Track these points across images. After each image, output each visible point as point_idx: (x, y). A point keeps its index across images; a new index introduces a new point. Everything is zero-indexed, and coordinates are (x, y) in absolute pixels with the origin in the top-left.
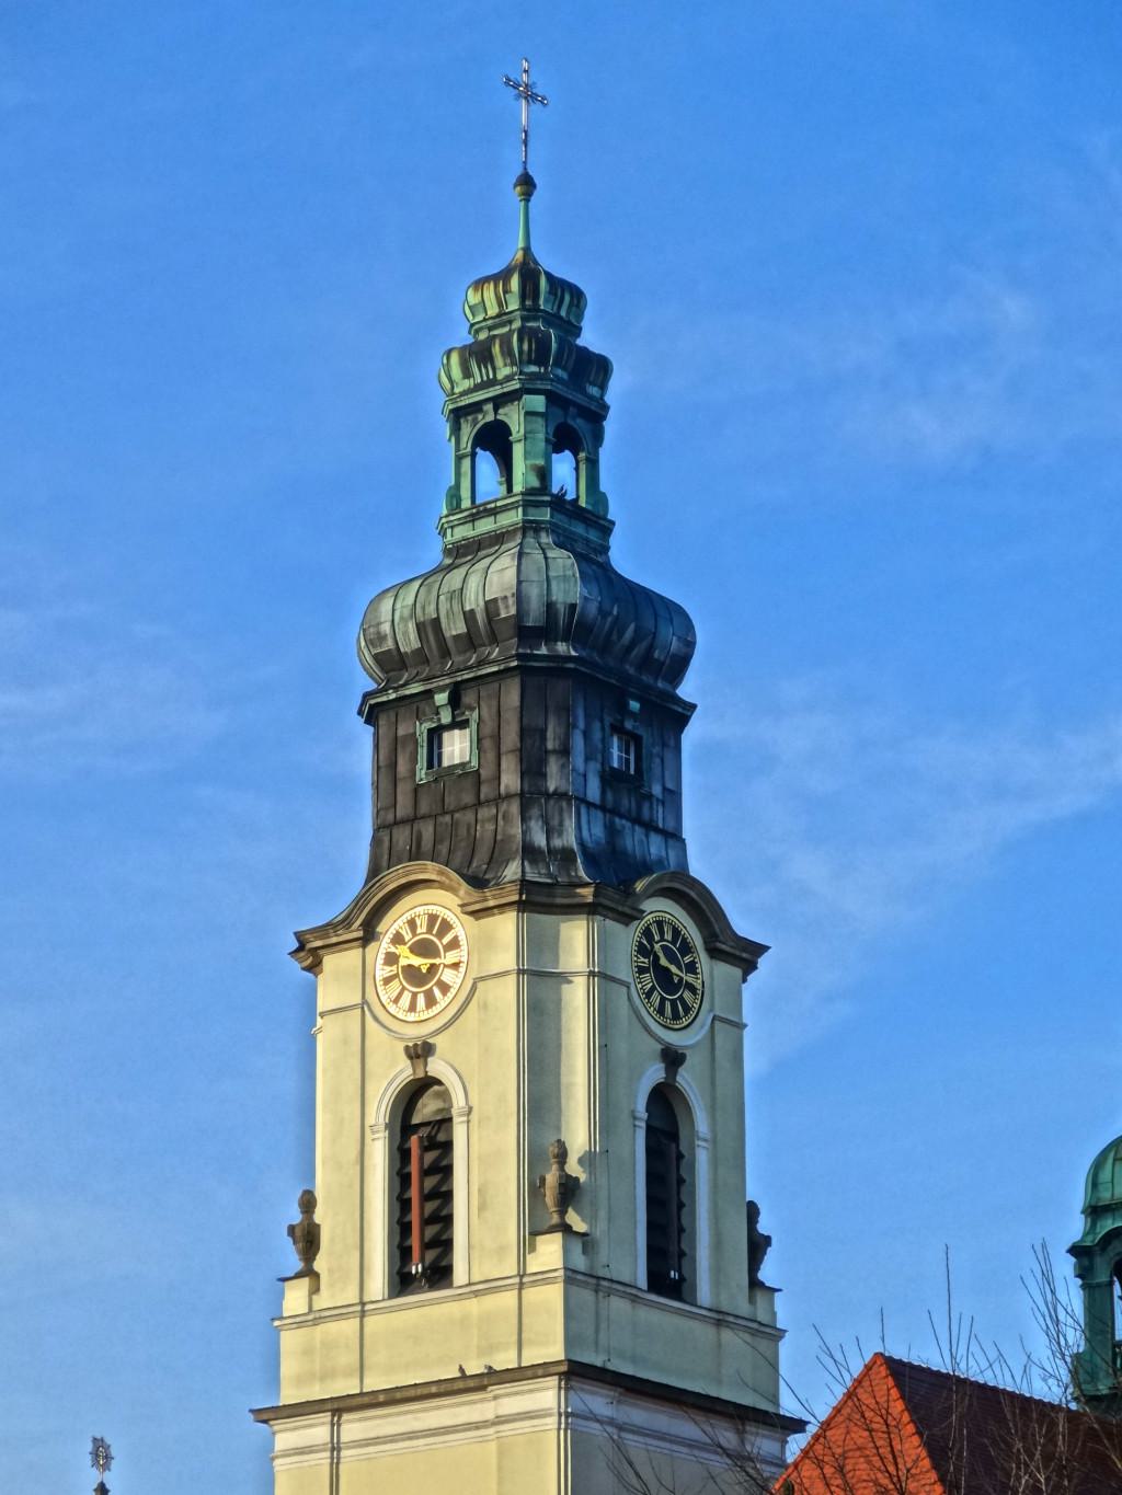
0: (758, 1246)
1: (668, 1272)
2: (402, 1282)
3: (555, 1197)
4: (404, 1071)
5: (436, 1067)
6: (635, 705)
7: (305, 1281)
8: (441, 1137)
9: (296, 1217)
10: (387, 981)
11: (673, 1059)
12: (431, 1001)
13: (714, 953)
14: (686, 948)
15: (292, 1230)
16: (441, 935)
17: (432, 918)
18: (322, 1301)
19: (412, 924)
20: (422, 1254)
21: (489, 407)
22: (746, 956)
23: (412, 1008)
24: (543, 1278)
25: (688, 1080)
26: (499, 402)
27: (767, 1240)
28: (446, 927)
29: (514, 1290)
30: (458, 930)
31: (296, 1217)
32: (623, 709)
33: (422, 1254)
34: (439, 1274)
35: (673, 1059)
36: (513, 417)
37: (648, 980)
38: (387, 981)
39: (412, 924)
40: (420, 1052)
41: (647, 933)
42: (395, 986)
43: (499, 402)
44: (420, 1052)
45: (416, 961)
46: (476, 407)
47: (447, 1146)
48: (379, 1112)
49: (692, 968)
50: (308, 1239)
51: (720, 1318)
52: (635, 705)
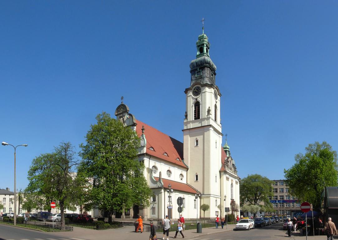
2: (195, 119)
11: (216, 102)
13: (219, 95)
20: (197, 116)
28: (199, 88)
32: (212, 72)
33: (197, 116)
34: (199, 118)
35: (216, 102)
40: (196, 99)
46: (200, 46)
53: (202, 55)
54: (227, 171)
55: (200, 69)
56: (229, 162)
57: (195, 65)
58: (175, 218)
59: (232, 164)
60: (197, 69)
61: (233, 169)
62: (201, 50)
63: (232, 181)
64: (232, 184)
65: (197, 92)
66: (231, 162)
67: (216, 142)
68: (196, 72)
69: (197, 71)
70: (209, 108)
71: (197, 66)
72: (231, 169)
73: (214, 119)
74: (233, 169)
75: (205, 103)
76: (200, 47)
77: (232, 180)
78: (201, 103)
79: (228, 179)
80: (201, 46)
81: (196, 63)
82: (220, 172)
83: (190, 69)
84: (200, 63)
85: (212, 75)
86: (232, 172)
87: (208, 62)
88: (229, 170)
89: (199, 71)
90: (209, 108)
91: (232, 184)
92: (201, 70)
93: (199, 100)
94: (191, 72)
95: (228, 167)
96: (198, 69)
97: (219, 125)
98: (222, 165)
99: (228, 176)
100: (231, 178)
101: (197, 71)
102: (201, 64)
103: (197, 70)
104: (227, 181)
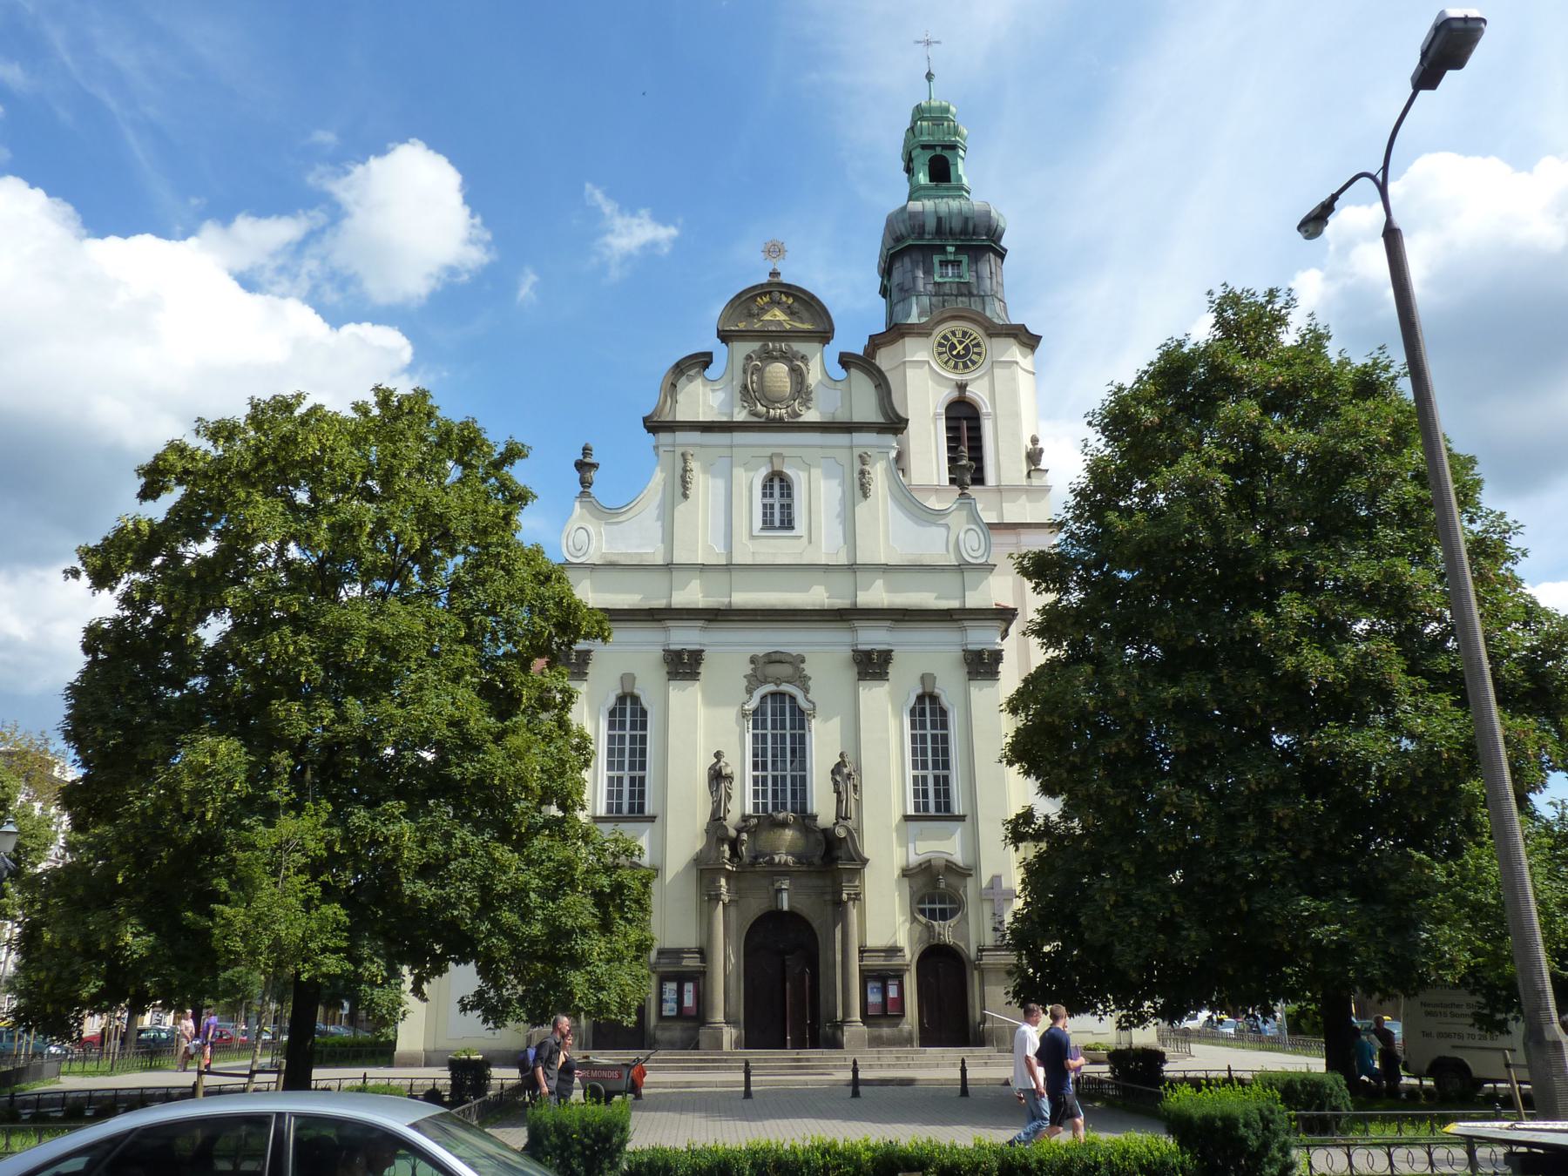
4: (955, 394)
17: (964, 334)
21: (939, 150)
40: (962, 387)
42: (945, 358)
43: (945, 147)
46: (932, 147)
53: (933, 192)
55: (957, 247)
57: (931, 224)
60: (942, 249)
62: (941, 171)
69: (943, 258)
70: (1035, 441)
71: (939, 230)
75: (1016, 415)
76: (929, 154)
78: (985, 408)
80: (939, 150)
81: (939, 219)
89: (951, 258)
90: (1035, 441)
92: (964, 259)
93: (977, 391)
101: (943, 258)
102: (964, 231)
103: (942, 249)
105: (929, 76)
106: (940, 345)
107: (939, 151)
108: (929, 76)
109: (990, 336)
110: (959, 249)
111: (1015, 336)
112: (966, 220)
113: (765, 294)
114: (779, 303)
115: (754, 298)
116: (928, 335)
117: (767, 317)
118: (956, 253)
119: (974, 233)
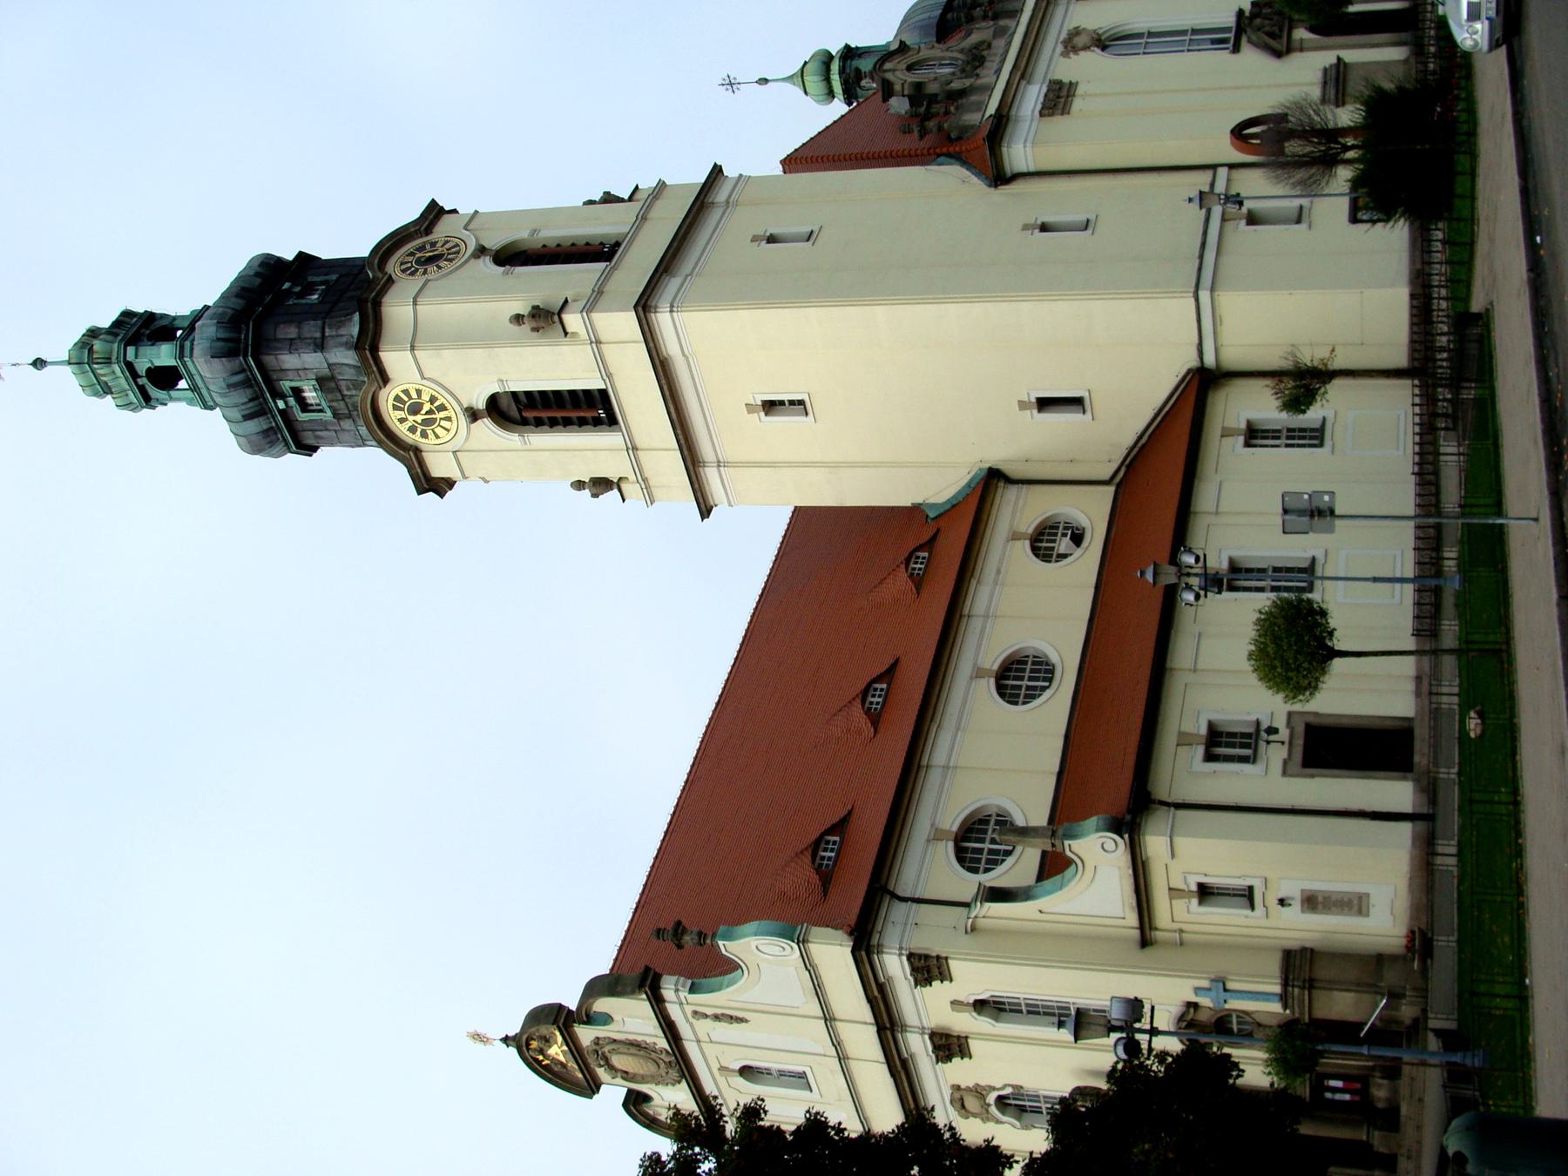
0: (609, 198)
1: (601, 252)
2: (612, 421)
3: (544, 319)
4: (486, 426)
5: (481, 404)
6: (287, 285)
7: (624, 486)
8: (523, 399)
9: (587, 493)
10: (437, 437)
11: (481, 251)
12: (442, 408)
13: (428, 231)
14: (422, 248)
15: (595, 495)
16: (404, 403)
17: (395, 408)
18: (632, 477)
19: (402, 421)
20: (589, 409)
21: (140, 381)
22: (434, 212)
23: (448, 419)
24: (591, 327)
25: (494, 241)
26: (134, 375)
27: (607, 194)
28: (397, 398)
29: (598, 348)
30: (397, 391)
31: (587, 493)
33: (589, 409)
35: (481, 251)
36: (142, 366)
37: (432, 268)
38: (437, 437)
39: (402, 421)
40: (473, 415)
41: (404, 271)
42: (439, 431)
43: (134, 375)
44: (473, 415)
45: (419, 418)
46: (142, 389)
47: (528, 394)
48: (512, 439)
49: (433, 244)
50: (601, 485)
51: (642, 218)
52: (287, 285)
54: (992, 108)
55: (278, 394)
56: (918, 86)
57: (253, 426)
58: (1410, 686)
59: (938, 52)
60: (283, 413)
61: (975, 38)
63: (1080, 41)
64: (1102, 42)
65: (425, 411)
66: (925, 53)
67: (772, 239)
68: (303, 417)
72: (976, 59)
73: (604, 265)
74: (975, 38)
76: (154, 392)
77: (1071, 45)
79: (1059, 99)
80: (140, 381)
81: (247, 418)
82: (999, 177)
83: (293, 460)
84: (241, 396)
85: (309, 289)
86: (1001, 32)
87: (222, 335)
88: (986, 76)
89: (292, 401)
91: (1102, 42)
92: (286, 385)
94: (310, 450)
95: (962, 93)
96: (281, 404)
97: (644, 218)
98: (949, 155)
99: (1032, 96)
100: (1054, 65)
102: (248, 383)
104: (1077, 104)
105: (39, 363)
106: (424, 435)
107: (143, 381)
108: (39, 363)
109: (385, 380)
110: (278, 394)
111: (375, 349)
112: (229, 386)
113: (539, 1062)
114: (541, 1051)
115: (546, 1067)
116: (417, 451)
117: (562, 1058)
118: (283, 397)
119: (243, 371)
